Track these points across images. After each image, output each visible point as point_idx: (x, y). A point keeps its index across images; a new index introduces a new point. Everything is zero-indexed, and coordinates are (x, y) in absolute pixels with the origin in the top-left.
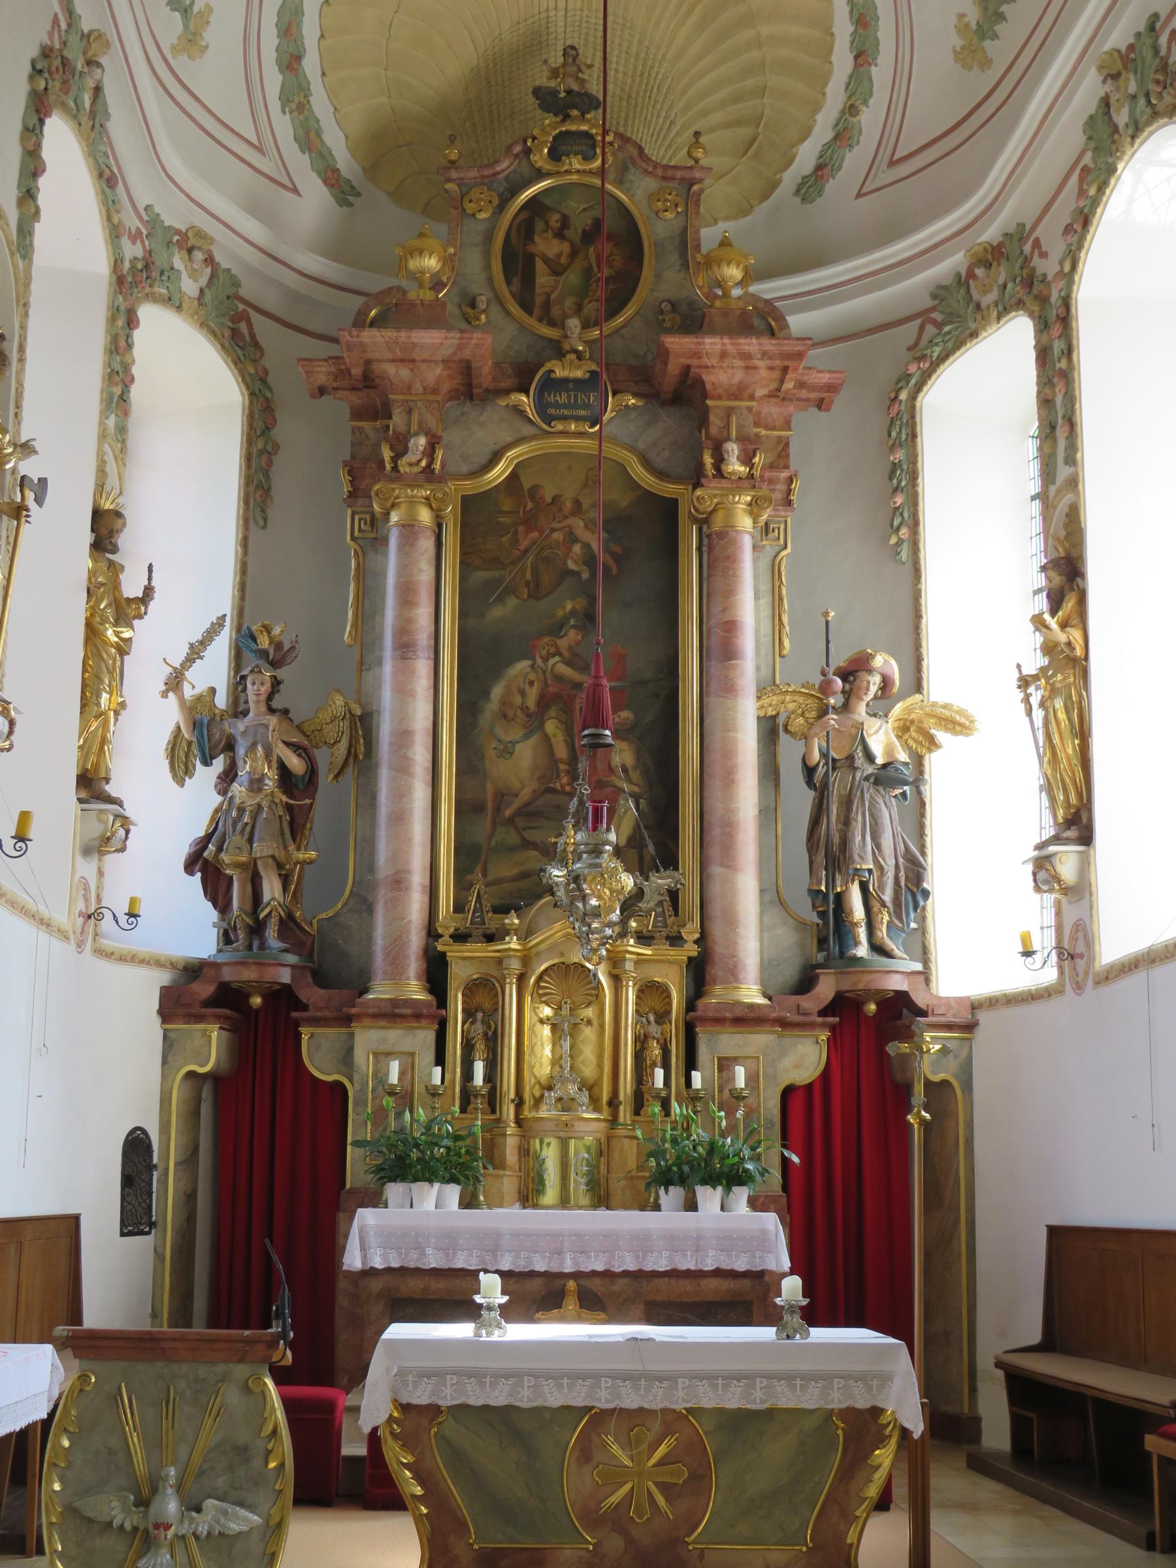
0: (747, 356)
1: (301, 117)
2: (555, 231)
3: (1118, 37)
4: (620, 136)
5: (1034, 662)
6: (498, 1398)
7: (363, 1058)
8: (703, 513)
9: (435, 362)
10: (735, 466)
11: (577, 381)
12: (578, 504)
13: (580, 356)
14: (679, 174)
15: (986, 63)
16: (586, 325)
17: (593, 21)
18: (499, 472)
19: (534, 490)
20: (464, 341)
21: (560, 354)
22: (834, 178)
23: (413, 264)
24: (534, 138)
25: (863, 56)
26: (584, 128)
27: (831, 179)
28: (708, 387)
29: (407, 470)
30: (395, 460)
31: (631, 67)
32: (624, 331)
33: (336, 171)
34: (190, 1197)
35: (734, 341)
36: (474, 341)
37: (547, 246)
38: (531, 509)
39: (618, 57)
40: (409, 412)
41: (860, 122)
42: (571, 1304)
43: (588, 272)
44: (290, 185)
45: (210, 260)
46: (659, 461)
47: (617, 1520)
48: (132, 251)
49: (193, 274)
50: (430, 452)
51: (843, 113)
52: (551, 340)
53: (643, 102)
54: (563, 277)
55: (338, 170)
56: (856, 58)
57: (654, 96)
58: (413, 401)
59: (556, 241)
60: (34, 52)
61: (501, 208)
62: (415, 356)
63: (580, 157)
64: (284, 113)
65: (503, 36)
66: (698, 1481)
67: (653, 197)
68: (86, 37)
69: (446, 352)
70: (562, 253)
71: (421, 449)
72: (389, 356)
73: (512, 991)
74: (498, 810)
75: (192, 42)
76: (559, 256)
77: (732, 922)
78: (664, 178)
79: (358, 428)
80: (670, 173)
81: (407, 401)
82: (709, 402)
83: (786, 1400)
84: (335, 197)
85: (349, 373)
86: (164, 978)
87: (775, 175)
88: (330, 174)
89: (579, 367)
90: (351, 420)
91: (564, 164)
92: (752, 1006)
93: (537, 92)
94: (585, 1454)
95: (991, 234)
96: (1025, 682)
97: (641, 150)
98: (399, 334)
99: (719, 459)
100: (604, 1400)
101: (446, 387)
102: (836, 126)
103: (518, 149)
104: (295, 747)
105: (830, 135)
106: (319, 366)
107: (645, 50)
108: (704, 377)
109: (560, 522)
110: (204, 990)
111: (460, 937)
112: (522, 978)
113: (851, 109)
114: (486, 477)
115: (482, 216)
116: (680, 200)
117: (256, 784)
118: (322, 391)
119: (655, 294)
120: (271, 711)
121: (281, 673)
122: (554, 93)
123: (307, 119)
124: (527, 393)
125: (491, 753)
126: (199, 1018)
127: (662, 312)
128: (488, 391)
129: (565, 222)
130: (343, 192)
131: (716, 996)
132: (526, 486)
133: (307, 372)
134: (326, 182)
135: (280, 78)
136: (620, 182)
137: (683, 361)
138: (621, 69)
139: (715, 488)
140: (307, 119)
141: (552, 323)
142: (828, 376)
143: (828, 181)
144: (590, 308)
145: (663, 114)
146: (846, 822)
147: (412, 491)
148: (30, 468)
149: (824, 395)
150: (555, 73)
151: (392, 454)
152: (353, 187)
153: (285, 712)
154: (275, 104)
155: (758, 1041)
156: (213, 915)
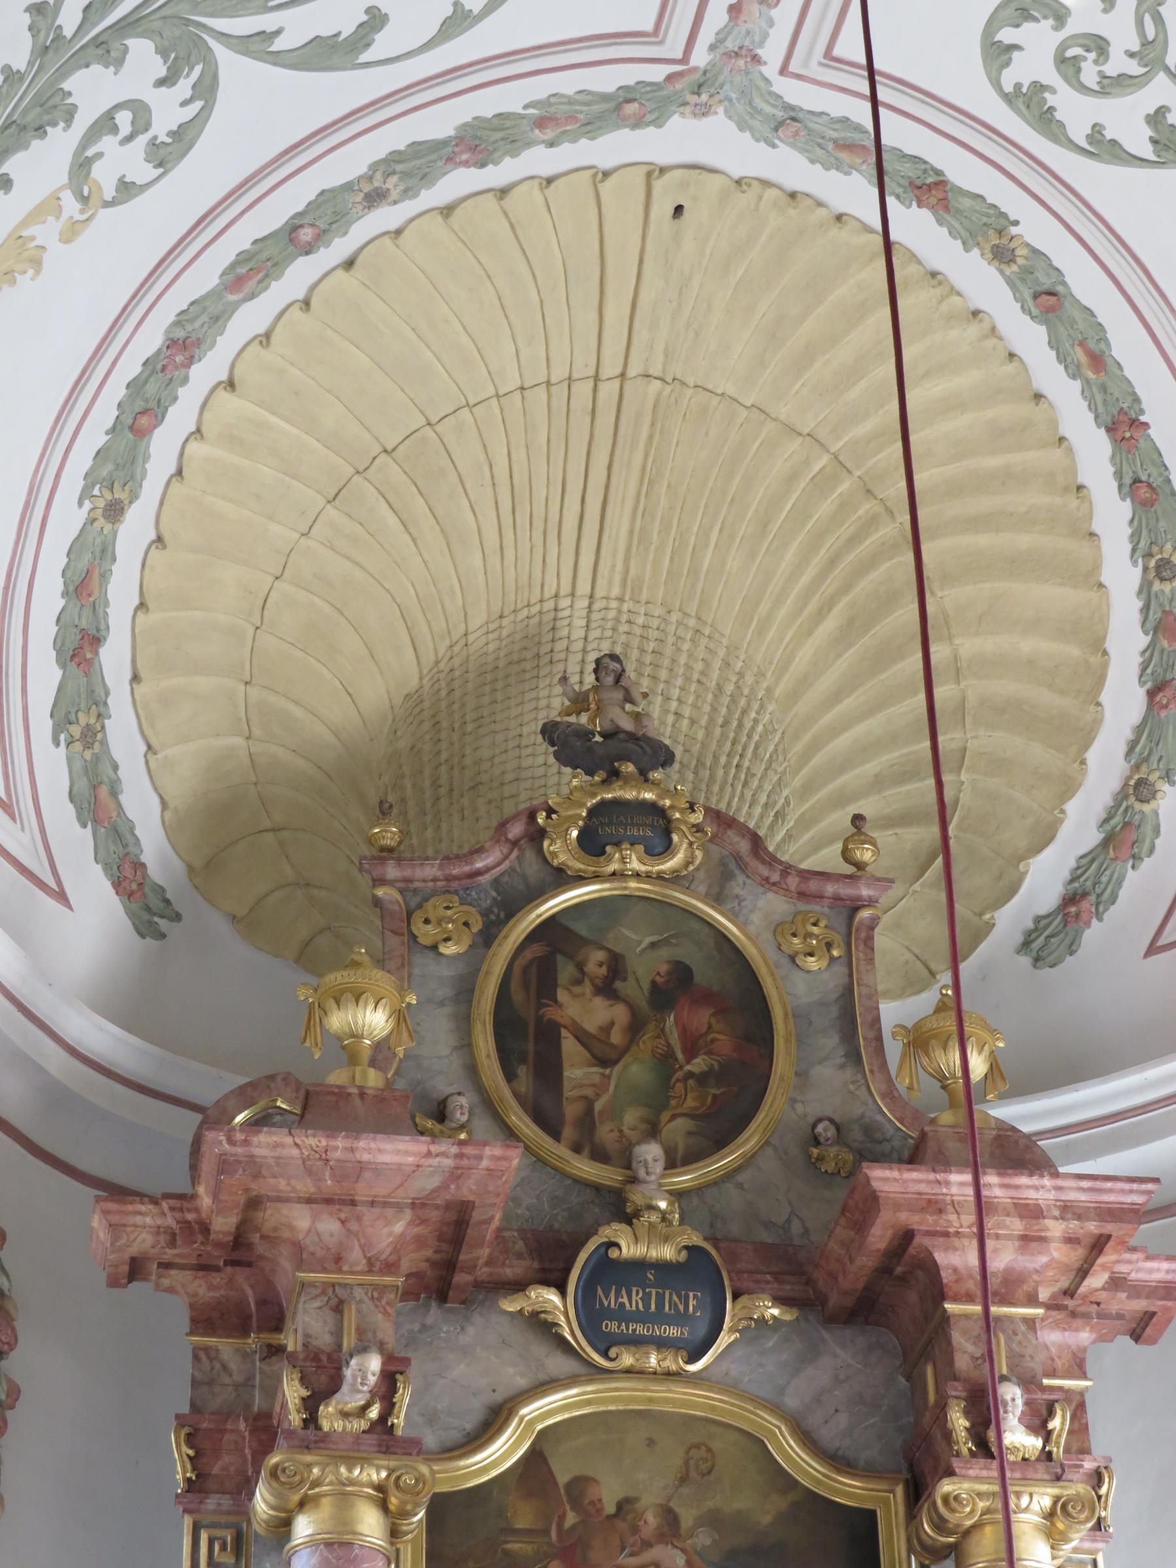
0: (1031, 1212)
1: (88, 755)
2: (598, 982)
4: (715, 815)
8: (950, 1533)
9: (399, 1207)
11: (662, 1267)
12: (670, 1518)
14: (830, 889)
16: (672, 1163)
17: (640, 620)
19: (579, 1486)
20: (465, 1162)
22: (1100, 919)
23: (337, 1020)
24: (550, 811)
26: (648, 796)
27: (1094, 921)
28: (946, 1276)
29: (338, 1425)
30: (311, 1405)
31: (707, 708)
32: (740, 1178)
33: (139, 866)
35: (1007, 1180)
36: (485, 1163)
38: (574, 1527)
39: (682, 689)
40: (338, 1309)
41: (1156, 813)
43: (665, 1062)
44: (52, 884)
46: (828, 1435)
51: (1121, 796)
52: (597, 1188)
53: (726, 774)
54: (618, 1068)
55: (143, 865)
56: (1151, 694)
57: (746, 763)
58: (344, 1286)
59: (599, 1002)
61: (488, 937)
62: (362, 1192)
63: (641, 848)
64: (57, 743)
65: (471, 638)
67: (781, 929)
69: (426, 1184)
70: (612, 1024)
71: (372, 1380)
72: (305, 1186)
76: (608, 1028)
78: (802, 895)
79: (206, 1349)
80: (813, 886)
81: (333, 1285)
82: (947, 1306)
84: (130, 914)
85: (205, 1229)
87: (981, 915)
88: (128, 871)
89: (666, 1239)
90: (191, 1333)
91: (610, 860)
93: (550, 731)
97: (756, 842)
98: (333, 1143)
101: (406, 1265)
102: (1106, 821)
103: (516, 830)
105: (1094, 837)
106: (140, 1213)
107: (734, 679)
108: (940, 1257)
109: (632, 1554)
114: (462, 1463)
115: (449, 949)
116: (838, 938)
118: (136, 1269)
119: (799, 1107)
122: (585, 735)
123: (97, 759)
124: (562, 1290)
127: (816, 1142)
128: (478, 1285)
129: (616, 966)
130: (148, 909)
132: (562, 1478)
133: (112, 1226)
134: (117, 885)
135: (58, 673)
136: (718, 899)
137: (905, 1218)
138: (687, 711)
139: (978, 1479)
140: (97, 759)
141: (600, 1155)
142: (1165, 1265)
143: (1088, 924)
144: (677, 1129)
145: (763, 799)
147: (350, 1470)
149: (1156, 1305)
150: (579, 702)
151: (305, 1393)
152: (167, 902)
154: (42, 725)
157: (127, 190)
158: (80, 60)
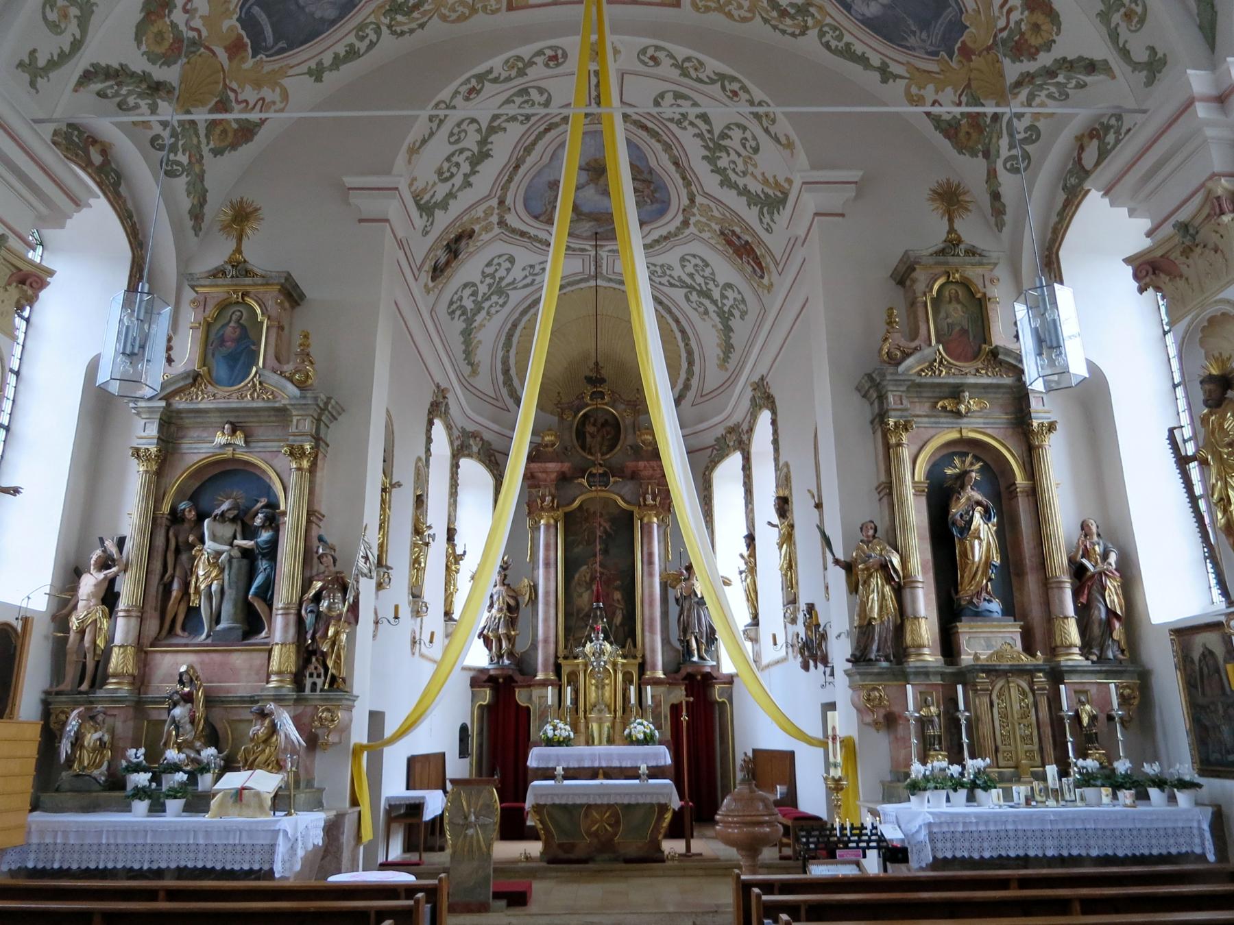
3: (756, 378)
5: (743, 567)
6: (563, 801)
7: (535, 698)
10: (650, 501)
13: (601, 465)
15: (727, 370)
16: (603, 454)
18: (576, 504)
19: (587, 510)
21: (595, 465)
25: (691, 363)
34: (480, 746)
37: (590, 429)
42: (601, 776)
43: (603, 437)
45: (482, 439)
46: (628, 498)
47: (595, 834)
48: (457, 443)
49: (476, 445)
50: (553, 501)
60: (428, 406)
66: (618, 822)
68: (443, 391)
73: (582, 675)
74: (578, 614)
75: (474, 373)
77: (653, 651)
83: (641, 801)
86: (472, 674)
92: (659, 678)
93: (586, 378)
94: (586, 816)
95: (731, 423)
96: (741, 573)
99: (645, 500)
100: (592, 801)
104: (512, 597)
105: (682, 386)
110: (485, 677)
111: (566, 658)
112: (585, 671)
113: (688, 379)
117: (500, 610)
120: (504, 584)
121: (507, 572)
125: (575, 595)
126: (483, 687)
131: (648, 674)
141: (592, 454)
144: (604, 449)
146: (688, 616)
148: (431, 532)
153: (508, 585)
155: (661, 690)
156: (487, 652)
157: (497, 312)
158: (483, 302)
